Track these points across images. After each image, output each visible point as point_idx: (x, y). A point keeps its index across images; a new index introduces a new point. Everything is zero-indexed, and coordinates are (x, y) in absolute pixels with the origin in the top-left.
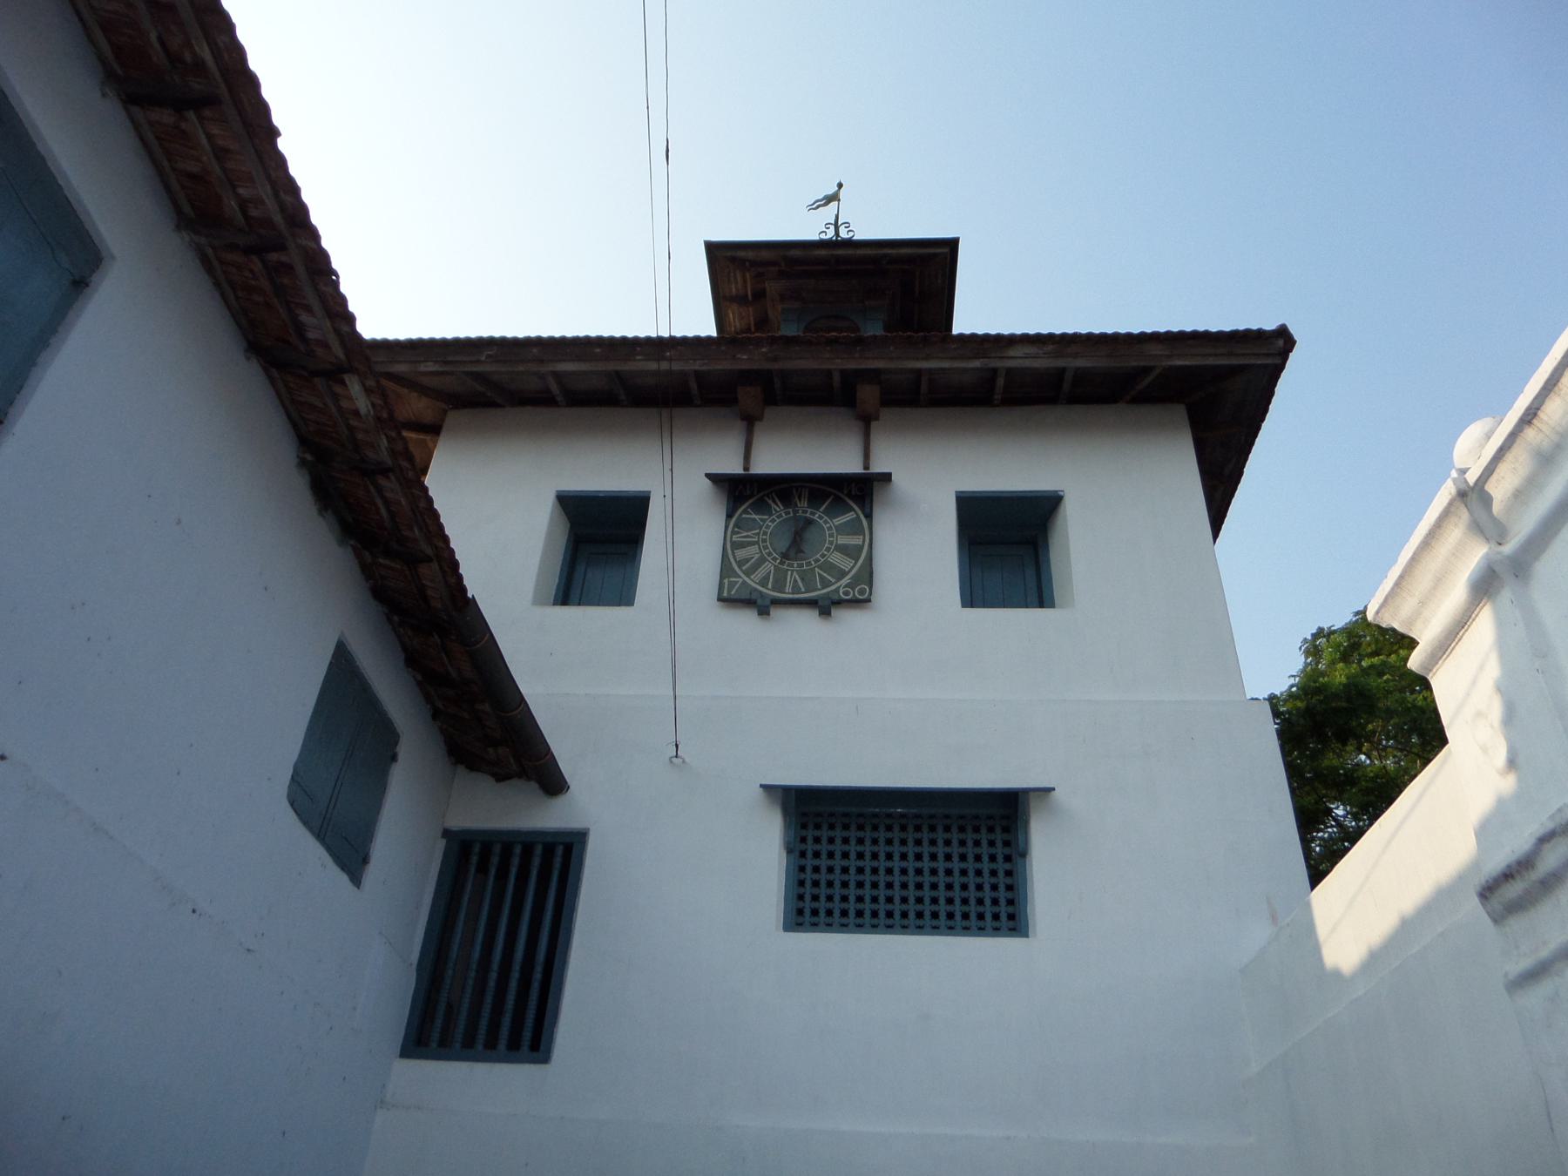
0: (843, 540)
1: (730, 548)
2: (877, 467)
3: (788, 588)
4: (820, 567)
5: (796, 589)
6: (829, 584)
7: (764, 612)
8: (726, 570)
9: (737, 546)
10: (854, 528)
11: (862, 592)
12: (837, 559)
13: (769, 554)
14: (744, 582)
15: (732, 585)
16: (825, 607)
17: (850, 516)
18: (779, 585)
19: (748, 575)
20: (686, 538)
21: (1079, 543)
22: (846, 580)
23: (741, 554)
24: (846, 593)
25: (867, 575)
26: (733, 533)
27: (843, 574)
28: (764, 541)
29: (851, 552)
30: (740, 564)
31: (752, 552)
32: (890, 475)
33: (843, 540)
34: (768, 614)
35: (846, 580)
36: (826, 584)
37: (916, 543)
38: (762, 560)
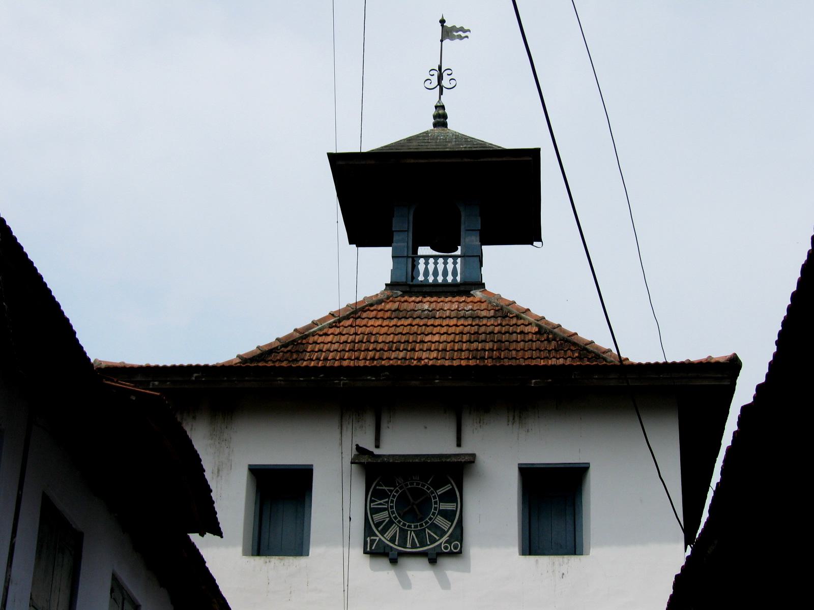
0: (444, 506)
1: (370, 511)
2: (465, 449)
3: (409, 545)
4: (429, 528)
5: (414, 546)
6: (436, 541)
7: (394, 562)
8: (368, 531)
9: (375, 511)
10: (450, 497)
11: (456, 548)
12: (440, 521)
13: (395, 518)
14: (380, 539)
15: (372, 541)
16: (433, 558)
17: (447, 488)
18: (403, 544)
19: (383, 532)
20: (337, 503)
21: (599, 500)
22: (445, 538)
23: (378, 517)
24: (446, 548)
25: (459, 535)
26: (372, 501)
27: (444, 533)
28: (392, 507)
29: (448, 515)
30: (377, 525)
31: (383, 516)
32: (474, 455)
33: (444, 506)
34: (397, 562)
35: (445, 538)
36: (433, 541)
37: (493, 507)
38: (391, 523)
